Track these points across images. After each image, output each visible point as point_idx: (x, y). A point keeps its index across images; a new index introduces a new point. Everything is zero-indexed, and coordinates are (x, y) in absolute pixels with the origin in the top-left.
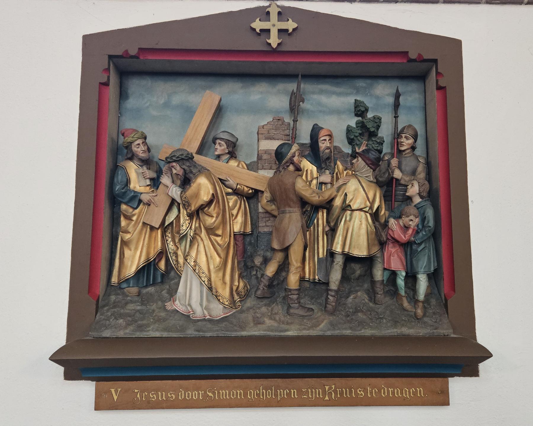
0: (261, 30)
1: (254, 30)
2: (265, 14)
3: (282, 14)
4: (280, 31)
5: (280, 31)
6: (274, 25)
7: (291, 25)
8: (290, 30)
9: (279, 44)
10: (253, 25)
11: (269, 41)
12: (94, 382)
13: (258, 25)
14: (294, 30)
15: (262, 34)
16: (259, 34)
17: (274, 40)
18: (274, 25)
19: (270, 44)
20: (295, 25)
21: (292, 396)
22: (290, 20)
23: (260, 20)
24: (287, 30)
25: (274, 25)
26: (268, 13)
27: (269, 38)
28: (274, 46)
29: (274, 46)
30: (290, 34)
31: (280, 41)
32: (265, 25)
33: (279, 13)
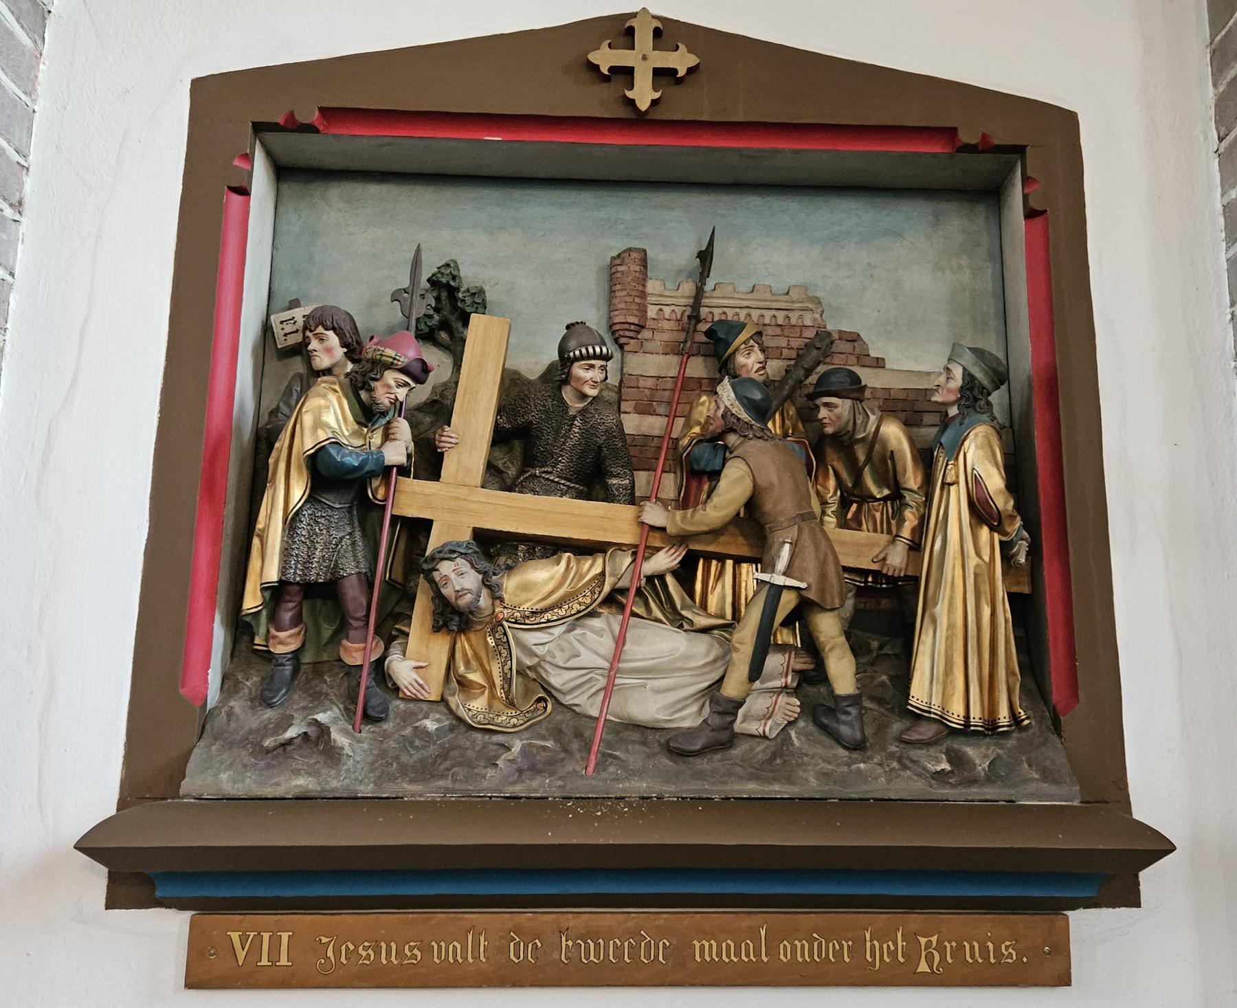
0: (611, 69)
1: (595, 68)
2: (621, 30)
3: (667, 33)
4: (658, 72)
5: (658, 72)
6: (644, 59)
7: (681, 61)
8: (681, 73)
9: (654, 103)
10: (594, 57)
11: (629, 94)
12: (187, 916)
13: (605, 58)
14: (691, 71)
15: (613, 77)
16: (606, 79)
17: (643, 93)
18: (645, 58)
19: (631, 103)
20: (693, 60)
21: (698, 959)
22: (682, 47)
23: (610, 46)
24: (675, 71)
25: (644, 59)
26: (630, 32)
27: (631, 87)
28: (643, 105)
29: (643, 105)
30: (680, 81)
31: (657, 95)
32: (623, 58)
33: (657, 33)
